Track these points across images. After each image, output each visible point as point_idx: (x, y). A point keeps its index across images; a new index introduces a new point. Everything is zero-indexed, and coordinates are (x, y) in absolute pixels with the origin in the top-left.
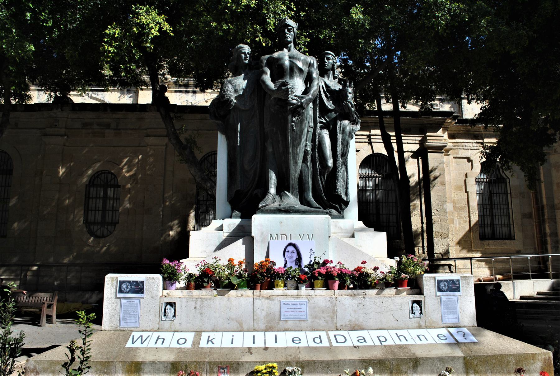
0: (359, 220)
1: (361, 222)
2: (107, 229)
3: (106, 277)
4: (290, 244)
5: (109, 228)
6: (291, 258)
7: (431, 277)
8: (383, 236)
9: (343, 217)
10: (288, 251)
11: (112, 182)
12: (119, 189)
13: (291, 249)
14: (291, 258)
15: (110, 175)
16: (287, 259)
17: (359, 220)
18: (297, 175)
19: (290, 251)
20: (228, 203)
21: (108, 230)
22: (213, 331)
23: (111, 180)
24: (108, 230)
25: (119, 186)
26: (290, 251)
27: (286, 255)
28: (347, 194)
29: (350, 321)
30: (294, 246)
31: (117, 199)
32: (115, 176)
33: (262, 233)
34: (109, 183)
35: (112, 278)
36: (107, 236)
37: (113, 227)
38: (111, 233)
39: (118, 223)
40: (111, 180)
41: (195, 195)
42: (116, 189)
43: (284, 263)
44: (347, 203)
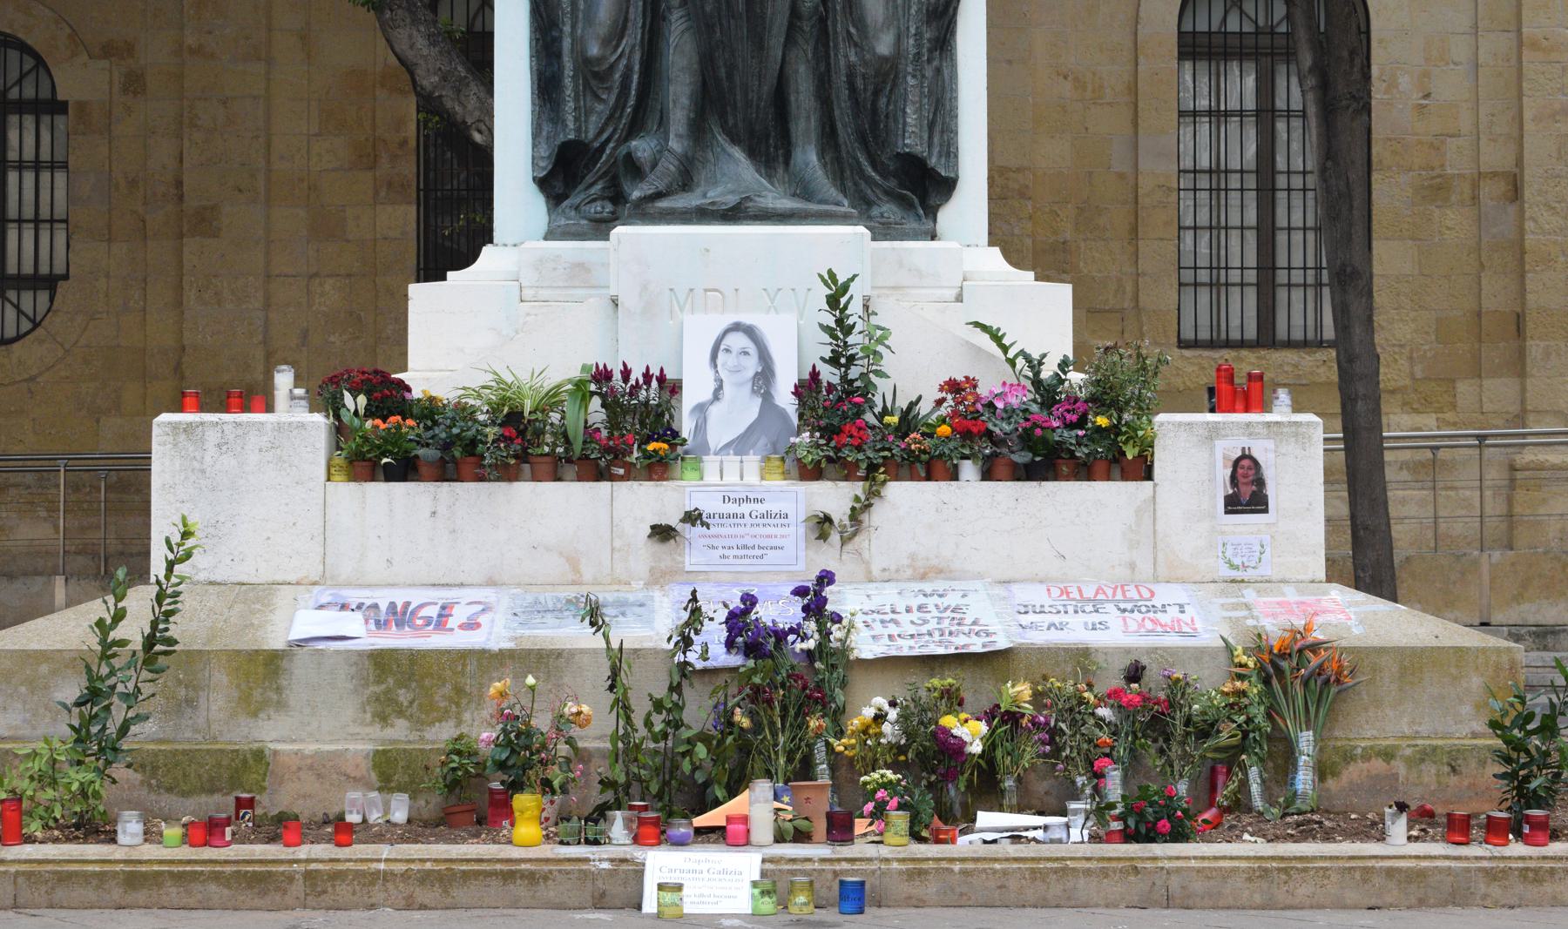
0: (991, 243)
1: (996, 250)
2: (17, 307)
3: (157, 420)
4: (736, 327)
5: (27, 299)
6: (736, 371)
7: (1180, 424)
8: (1062, 294)
9: (933, 237)
10: (727, 350)
11: (29, 92)
12: (60, 121)
13: (738, 341)
14: (736, 371)
15: (13, 55)
16: (723, 375)
17: (991, 243)
18: (767, 88)
20: (533, 188)
21: (20, 311)
22: (491, 583)
23: (22, 77)
24: (20, 311)
25: (60, 108)
27: (719, 362)
28: (950, 152)
29: (913, 557)
30: (750, 331)
31: (53, 166)
32: (40, 62)
33: (645, 288)
34: (14, 94)
35: (175, 427)
36: (19, 338)
37: (43, 297)
38: (36, 325)
39: (66, 277)
40: (22, 77)
41: (413, 143)
42: (46, 119)
43: (712, 386)
44: (947, 186)
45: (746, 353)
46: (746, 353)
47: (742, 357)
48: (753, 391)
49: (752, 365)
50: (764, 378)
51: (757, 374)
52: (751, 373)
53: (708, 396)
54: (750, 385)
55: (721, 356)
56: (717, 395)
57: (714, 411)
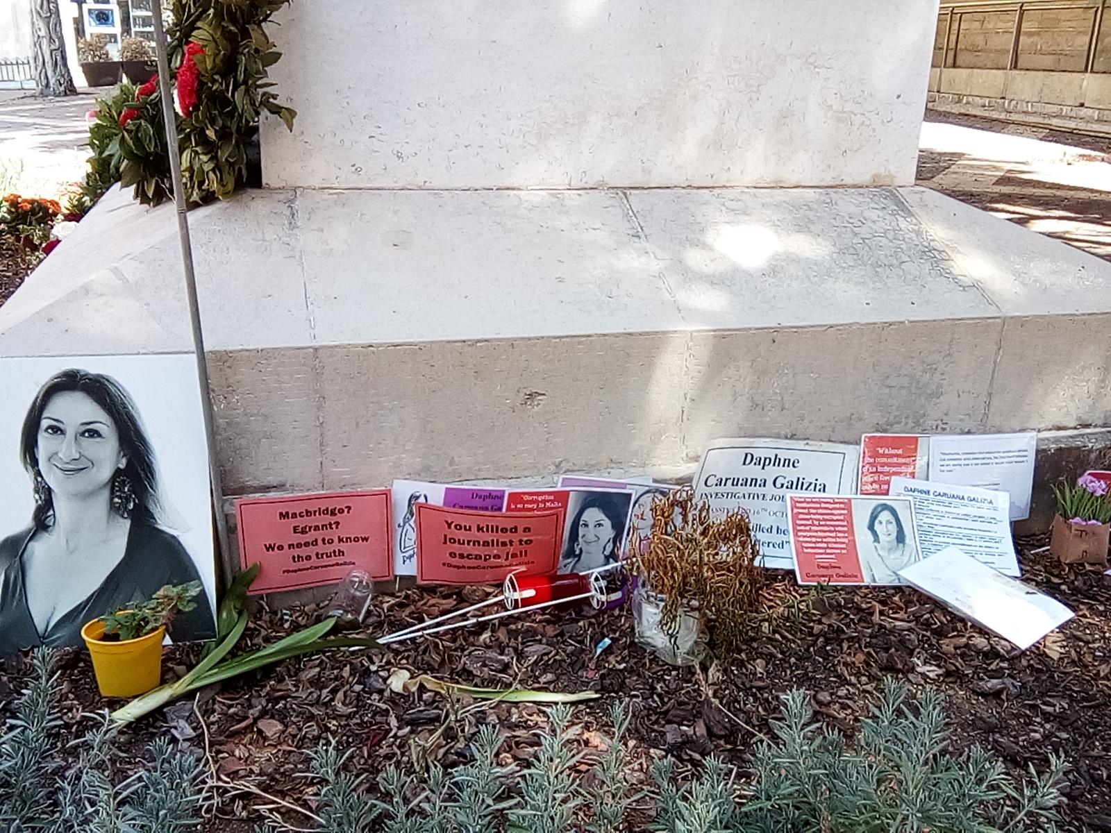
4: (70, 382)
6: (75, 469)
10: (56, 430)
13: (75, 410)
14: (75, 469)
16: (52, 479)
19: (71, 428)
26: (71, 428)
27: (42, 453)
30: (98, 389)
43: (29, 504)
45: (94, 434)
46: (94, 434)
47: (87, 442)
48: (115, 509)
49: (106, 456)
50: (134, 481)
51: (118, 472)
52: (106, 473)
53: (25, 521)
54: (106, 494)
55: (45, 443)
56: (42, 520)
57: (39, 551)
